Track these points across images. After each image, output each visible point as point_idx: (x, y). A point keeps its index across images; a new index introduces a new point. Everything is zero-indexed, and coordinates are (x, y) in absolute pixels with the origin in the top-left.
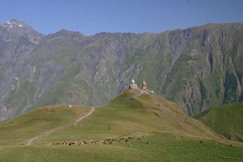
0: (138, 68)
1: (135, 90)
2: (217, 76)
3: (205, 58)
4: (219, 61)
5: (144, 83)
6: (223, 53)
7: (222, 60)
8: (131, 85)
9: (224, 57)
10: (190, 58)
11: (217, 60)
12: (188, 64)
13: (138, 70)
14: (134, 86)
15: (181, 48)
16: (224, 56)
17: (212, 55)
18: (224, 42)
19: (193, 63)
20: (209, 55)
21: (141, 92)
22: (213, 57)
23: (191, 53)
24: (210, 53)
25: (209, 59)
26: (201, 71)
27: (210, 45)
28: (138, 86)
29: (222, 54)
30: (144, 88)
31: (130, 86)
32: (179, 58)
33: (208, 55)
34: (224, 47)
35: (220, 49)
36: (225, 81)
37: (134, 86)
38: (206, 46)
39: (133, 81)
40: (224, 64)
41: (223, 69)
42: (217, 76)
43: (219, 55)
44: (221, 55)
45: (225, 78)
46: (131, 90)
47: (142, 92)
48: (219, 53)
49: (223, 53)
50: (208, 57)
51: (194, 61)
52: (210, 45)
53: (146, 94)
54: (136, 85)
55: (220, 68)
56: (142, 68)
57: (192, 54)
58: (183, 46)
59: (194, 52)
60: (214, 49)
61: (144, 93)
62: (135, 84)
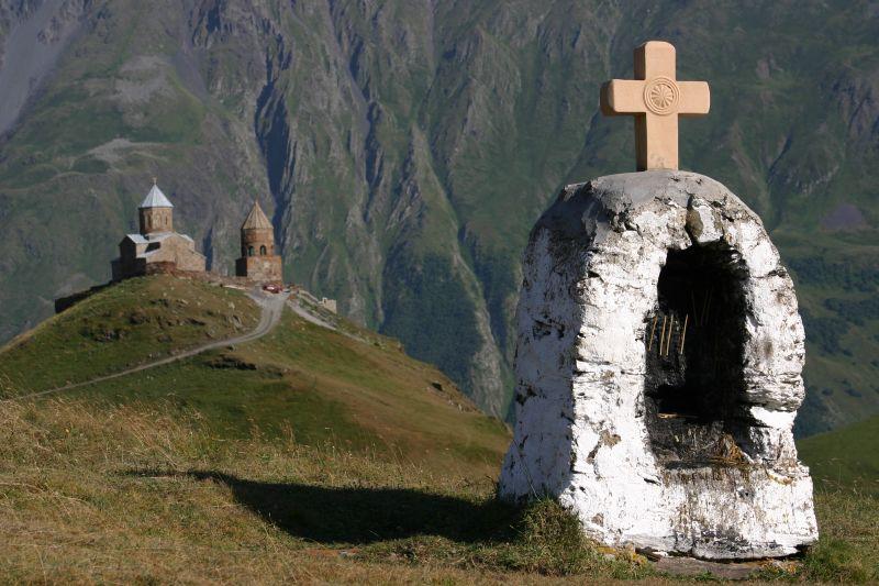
2: (322, 275)
3: (226, 125)
4: (337, 152)
6: (366, 93)
7: (357, 148)
9: (372, 130)
10: (113, 121)
11: (321, 147)
12: (101, 166)
15: (41, 36)
16: (373, 118)
17: (281, 105)
18: (370, 13)
19: (134, 161)
20: (261, 102)
22: (293, 125)
23: (121, 85)
24: (268, 90)
25: (260, 138)
26: (204, 225)
27: (266, 27)
29: (360, 104)
32: (21, 120)
33: (251, 102)
34: (368, 49)
35: (343, 61)
36: (381, 312)
38: (236, 33)
40: (373, 181)
41: (365, 216)
42: (322, 275)
43: (335, 106)
44: (353, 108)
45: (385, 287)
48: (337, 97)
49: (366, 93)
50: (249, 116)
51: (145, 150)
52: (266, 27)
55: (342, 214)
57: (129, 93)
58: (56, 26)
59: (141, 79)
60: (298, 57)
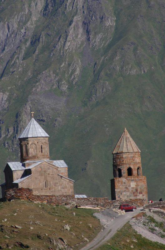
0: (78, 19)
1: (54, 204)
5: (129, 148)
8: (16, 166)
13: (75, 38)
14: (46, 174)
21: (99, 227)
28: (72, 173)
30: (127, 188)
31: (8, 172)
37: (43, 172)
39: (35, 131)
46: (20, 206)
47: (104, 220)
53: (143, 242)
54: (61, 164)
56: (110, 22)
61: (127, 231)
62: (54, 156)
